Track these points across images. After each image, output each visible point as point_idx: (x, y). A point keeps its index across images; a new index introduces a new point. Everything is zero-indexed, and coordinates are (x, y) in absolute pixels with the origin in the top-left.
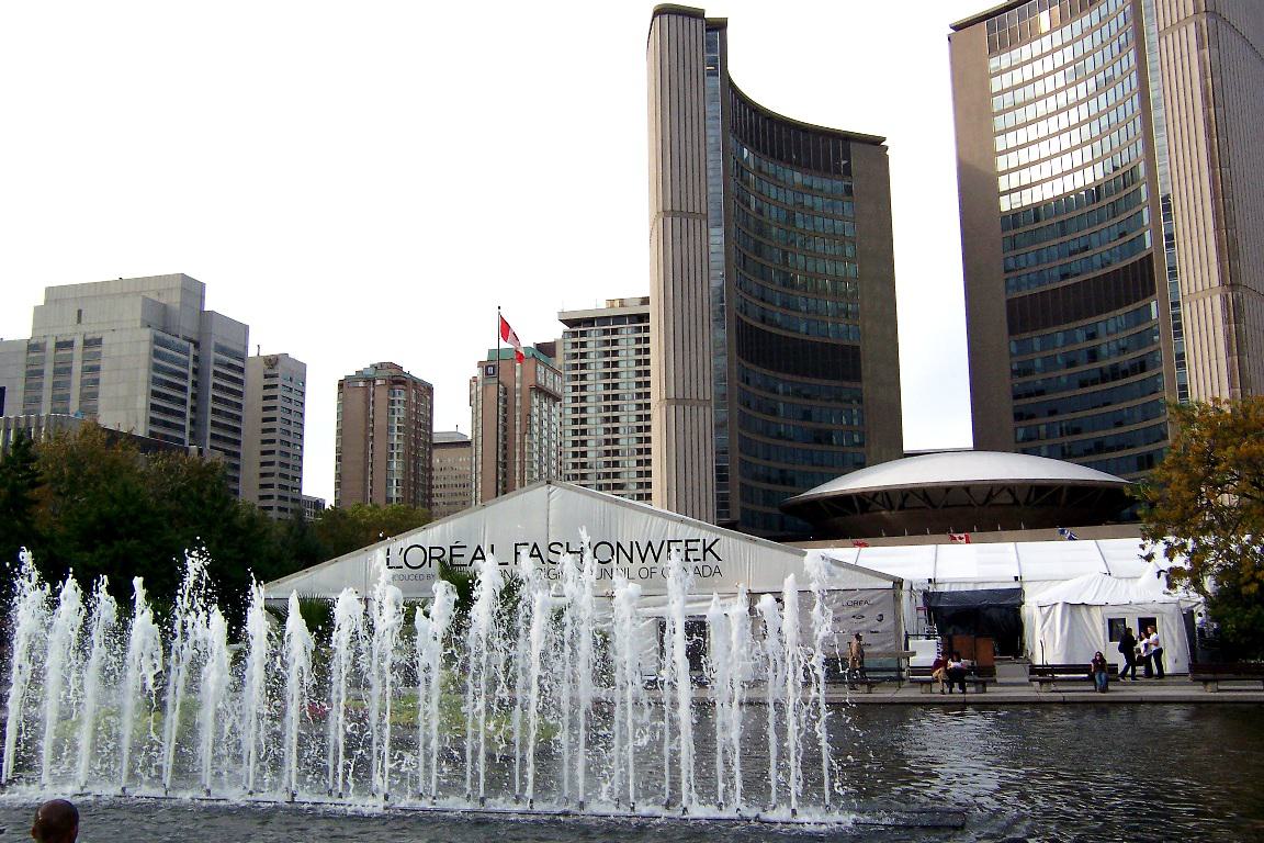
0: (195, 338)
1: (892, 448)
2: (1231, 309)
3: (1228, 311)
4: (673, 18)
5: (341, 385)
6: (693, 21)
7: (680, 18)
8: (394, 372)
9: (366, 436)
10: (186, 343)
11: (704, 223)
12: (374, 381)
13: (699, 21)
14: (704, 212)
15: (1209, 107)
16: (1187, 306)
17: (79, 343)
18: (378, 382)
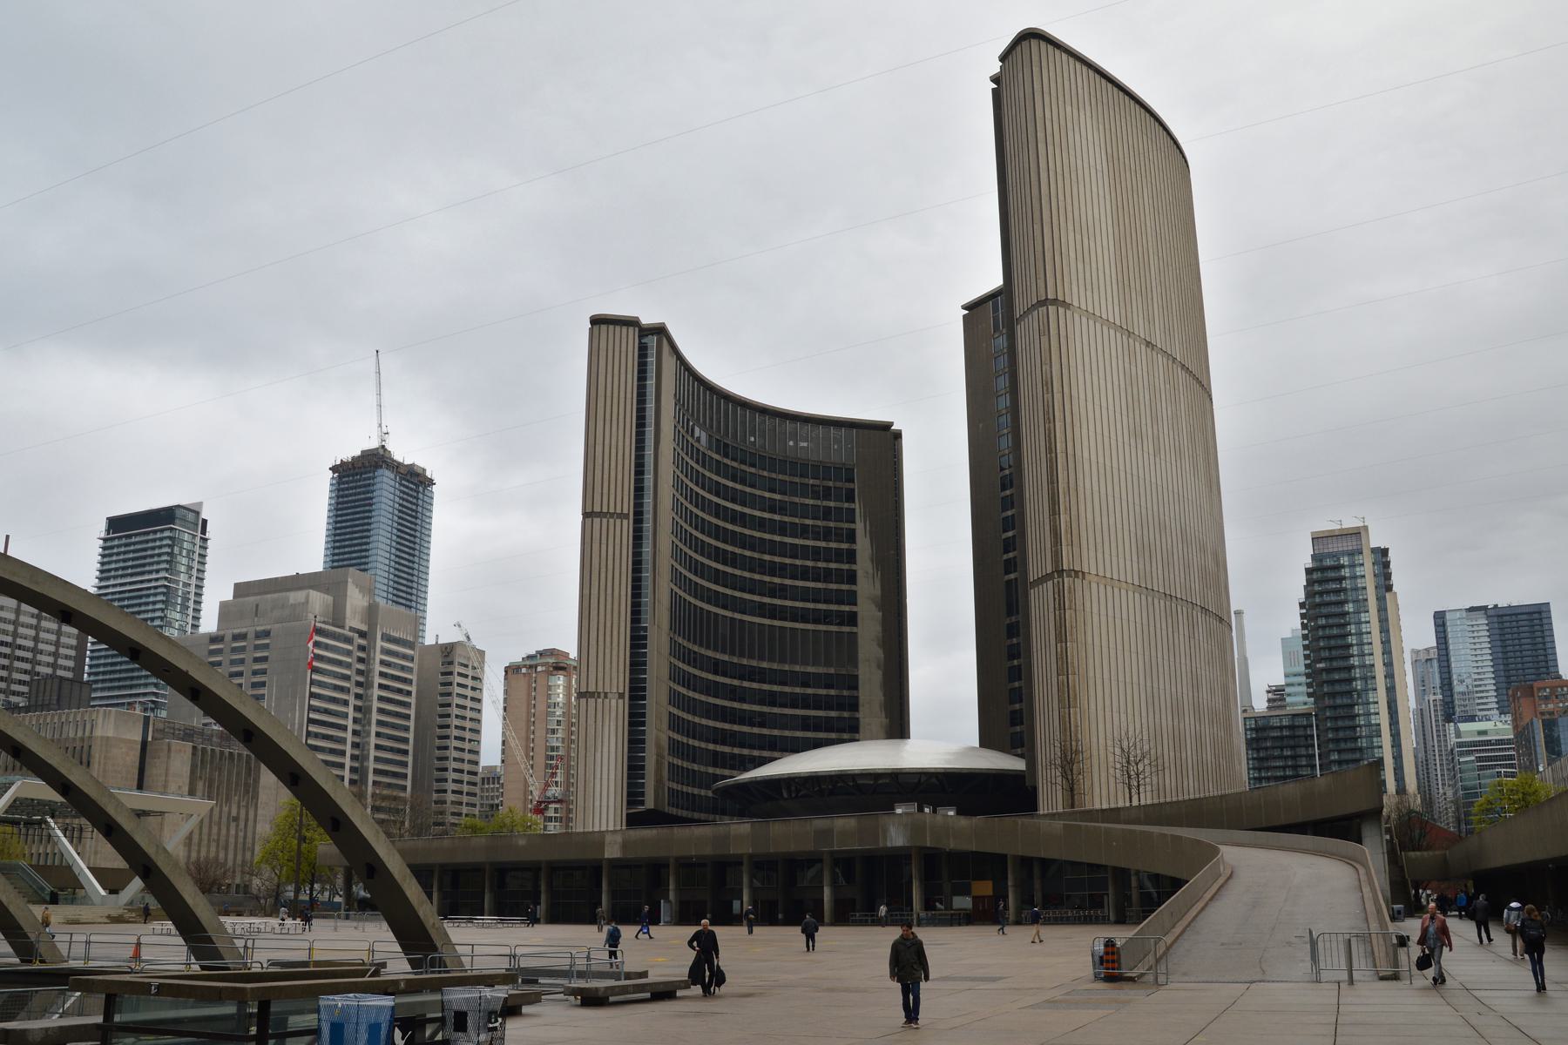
0: (364, 628)
1: (898, 728)
2: (1062, 594)
3: (1059, 596)
4: (604, 327)
5: (507, 670)
6: (624, 329)
7: (611, 327)
8: (551, 660)
9: (528, 721)
10: (351, 634)
11: (625, 522)
12: (536, 668)
13: (631, 329)
14: (625, 511)
15: (1048, 393)
16: (1032, 591)
17: (251, 636)
18: (539, 669)
